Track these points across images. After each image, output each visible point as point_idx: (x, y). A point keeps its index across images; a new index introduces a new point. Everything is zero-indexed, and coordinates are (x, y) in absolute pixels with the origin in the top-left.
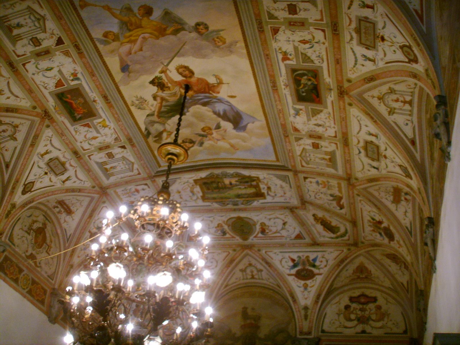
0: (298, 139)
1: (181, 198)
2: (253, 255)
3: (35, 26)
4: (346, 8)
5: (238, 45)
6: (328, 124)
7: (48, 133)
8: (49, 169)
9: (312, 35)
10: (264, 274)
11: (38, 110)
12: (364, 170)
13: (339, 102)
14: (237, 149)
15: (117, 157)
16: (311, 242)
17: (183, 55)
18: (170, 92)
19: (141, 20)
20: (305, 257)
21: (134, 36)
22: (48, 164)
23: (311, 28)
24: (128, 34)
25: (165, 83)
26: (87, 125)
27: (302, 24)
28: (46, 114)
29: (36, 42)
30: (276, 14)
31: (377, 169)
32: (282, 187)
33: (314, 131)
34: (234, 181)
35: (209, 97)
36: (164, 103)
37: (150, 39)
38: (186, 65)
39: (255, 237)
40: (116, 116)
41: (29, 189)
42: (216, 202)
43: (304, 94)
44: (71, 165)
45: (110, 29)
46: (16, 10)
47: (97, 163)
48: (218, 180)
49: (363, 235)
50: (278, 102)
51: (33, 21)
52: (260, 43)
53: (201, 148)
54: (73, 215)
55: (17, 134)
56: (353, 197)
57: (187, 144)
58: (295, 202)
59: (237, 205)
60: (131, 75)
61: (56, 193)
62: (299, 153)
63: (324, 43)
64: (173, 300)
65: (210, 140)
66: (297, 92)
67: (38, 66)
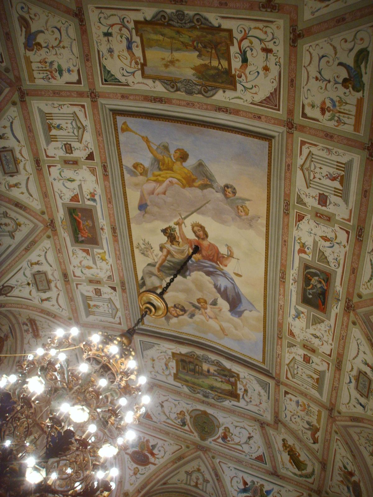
0: (291, 345)
1: (153, 367)
2: (205, 460)
3: (73, 133)
5: (260, 221)
6: (325, 338)
7: (47, 243)
8: (34, 281)
9: (336, 234)
10: (209, 488)
11: (46, 217)
12: (350, 404)
13: (344, 317)
14: (226, 335)
15: (104, 296)
16: (271, 470)
17: (203, 214)
18: (178, 248)
19: (174, 162)
20: (259, 484)
21: (163, 177)
22: (34, 275)
23: (336, 225)
24: (157, 173)
25: (177, 237)
26: (87, 252)
27: (329, 219)
28: (51, 224)
29: (69, 148)
30: (306, 200)
31: (364, 407)
32: (259, 395)
33: (310, 342)
34: (212, 369)
35: (213, 267)
36: (169, 258)
37: (176, 185)
38: (203, 225)
39: (215, 440)
40: (118, 253)
41: (6, 293)
42: (187, 386)
43: (311, 296)
44: (56, 287)
45: (142, 162)
46: (62, 111)
47: (82, 295)
48: (196, 362)
49: (330, 483)
50: (281, 297)
51: (73, 127)
52: (281, 226)
53: (190, 320)
54: (39, 339)
55: (17, 232)
56: (330, 433)
57: (178, 310)
58: (268, 417)
59: (207, 397)
60: (146, 215)
61: (31, 308)
62: (287, 362)
63: (345, 247)
64: (78, 438)
65: (202, 314)
66: (304, 291)
67: (62, 173)
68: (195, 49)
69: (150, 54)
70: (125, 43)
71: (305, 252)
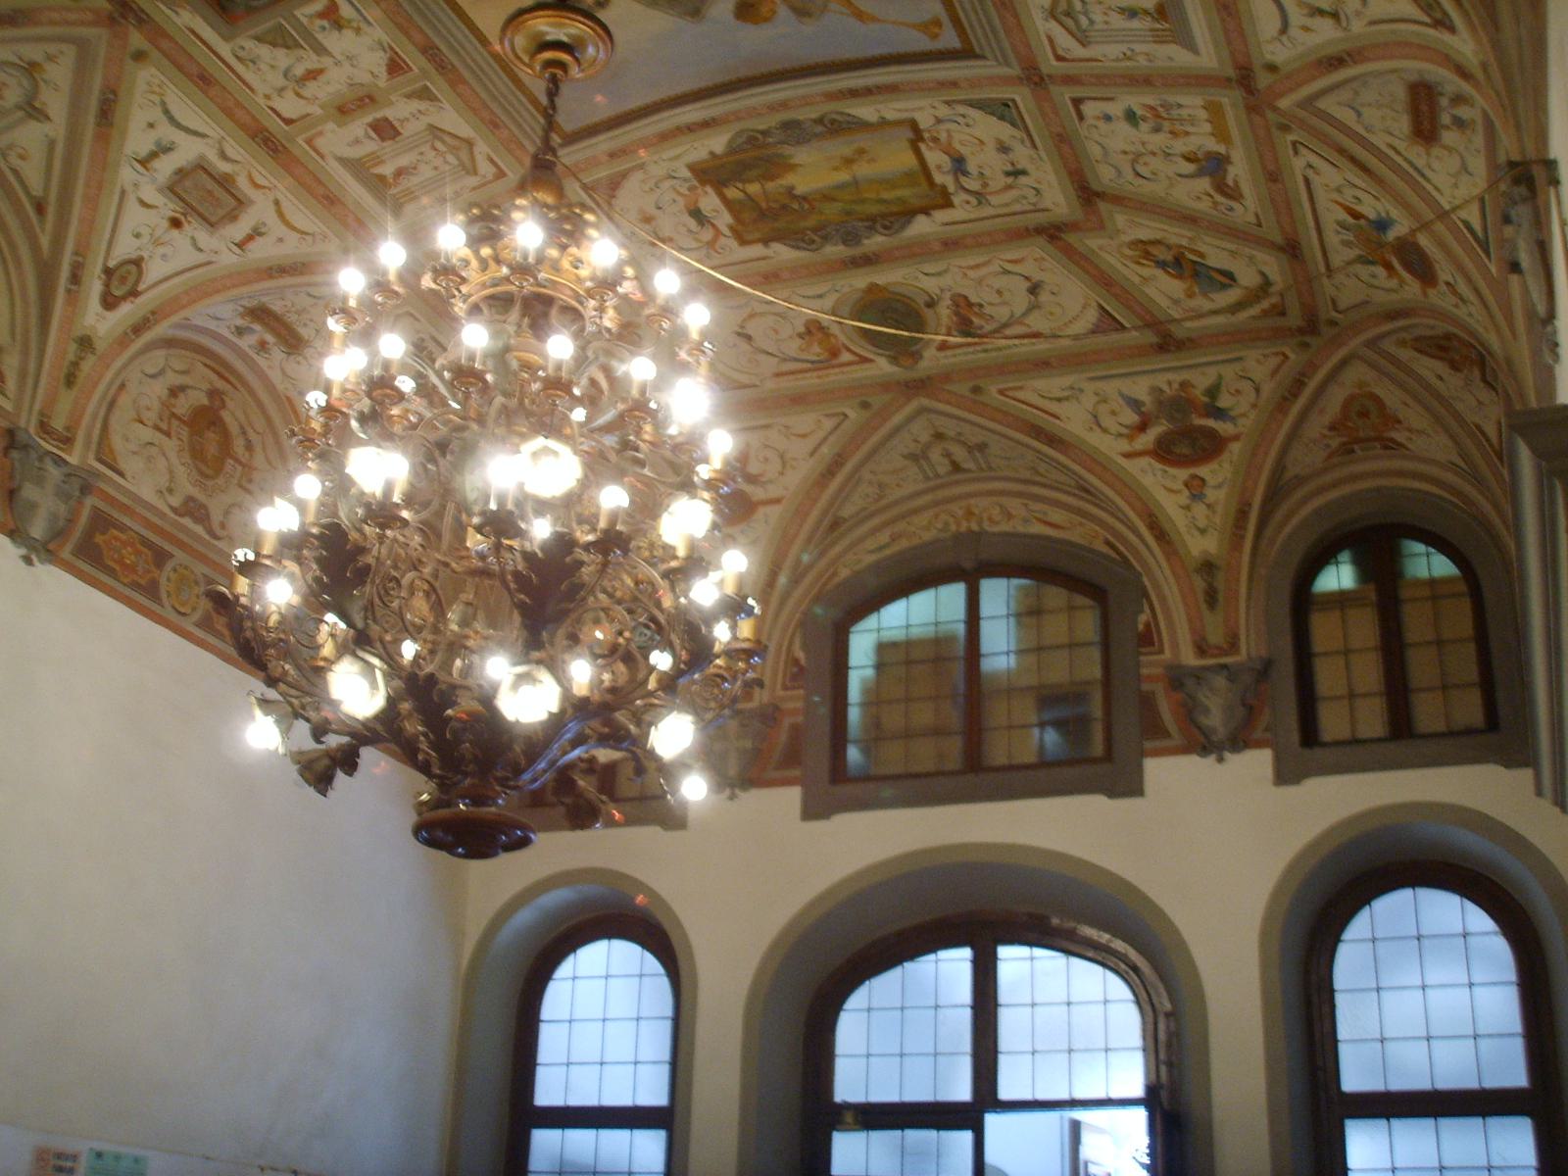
4: (280, 197)
30: (415, 105)
46: (1124, 48)
68: (805, 198)
69: (909, 160)
70: (972, 167)
71: (322, 15)
